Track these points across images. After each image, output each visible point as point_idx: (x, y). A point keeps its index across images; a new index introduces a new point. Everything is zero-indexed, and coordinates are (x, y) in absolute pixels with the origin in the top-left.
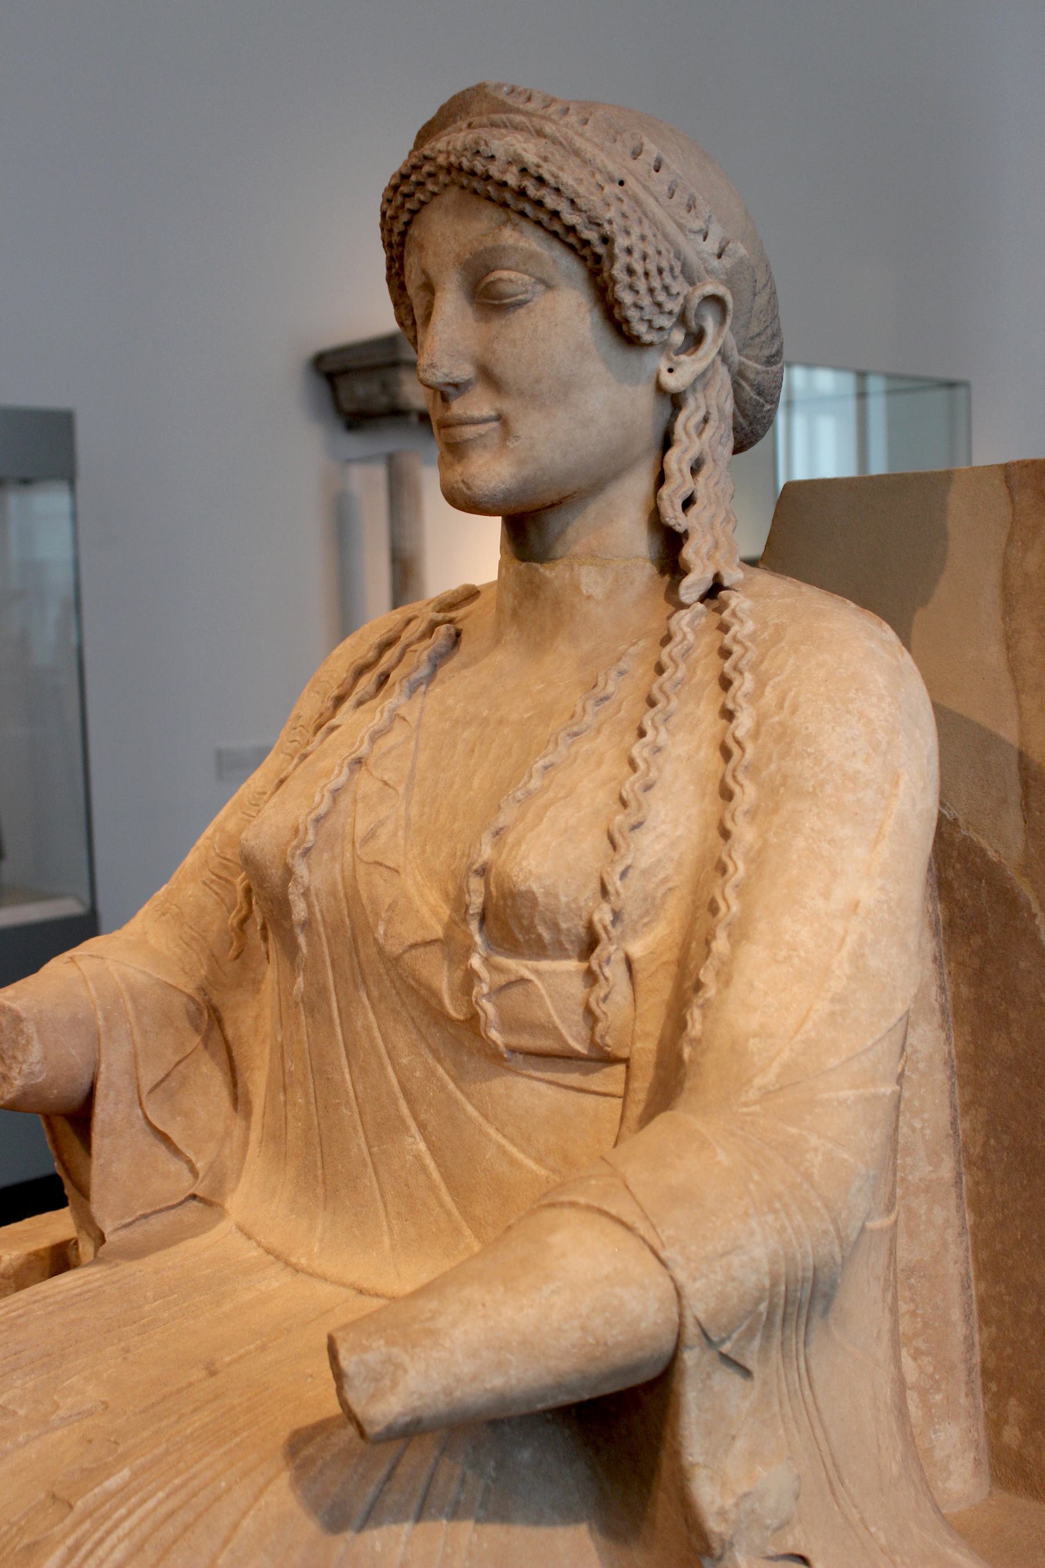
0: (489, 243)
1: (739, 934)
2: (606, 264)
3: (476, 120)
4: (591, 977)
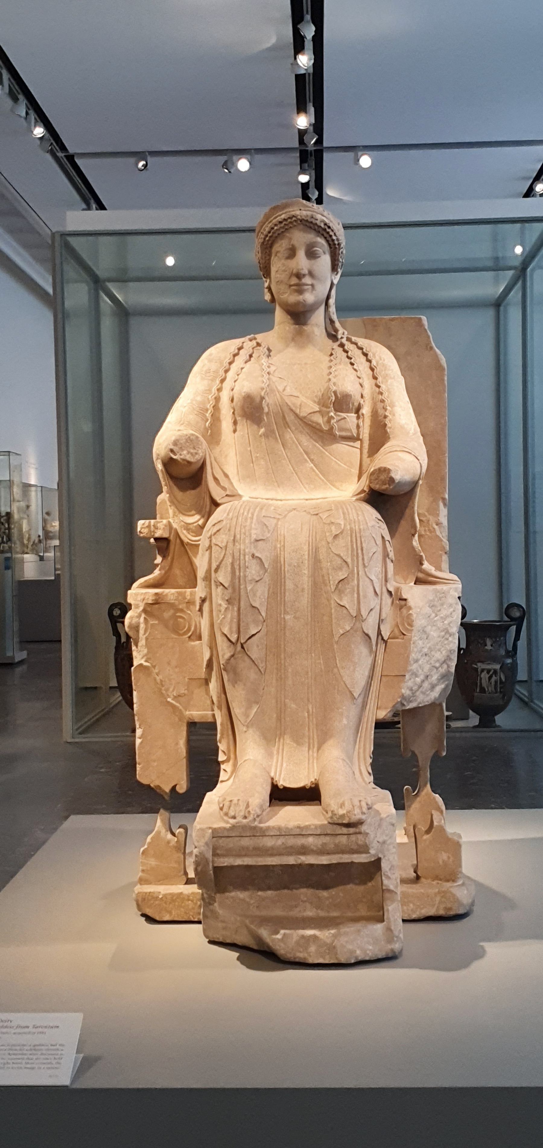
0: (314, 240)
1: (392, 406)
3: (302, 208)
4: (358, 418)
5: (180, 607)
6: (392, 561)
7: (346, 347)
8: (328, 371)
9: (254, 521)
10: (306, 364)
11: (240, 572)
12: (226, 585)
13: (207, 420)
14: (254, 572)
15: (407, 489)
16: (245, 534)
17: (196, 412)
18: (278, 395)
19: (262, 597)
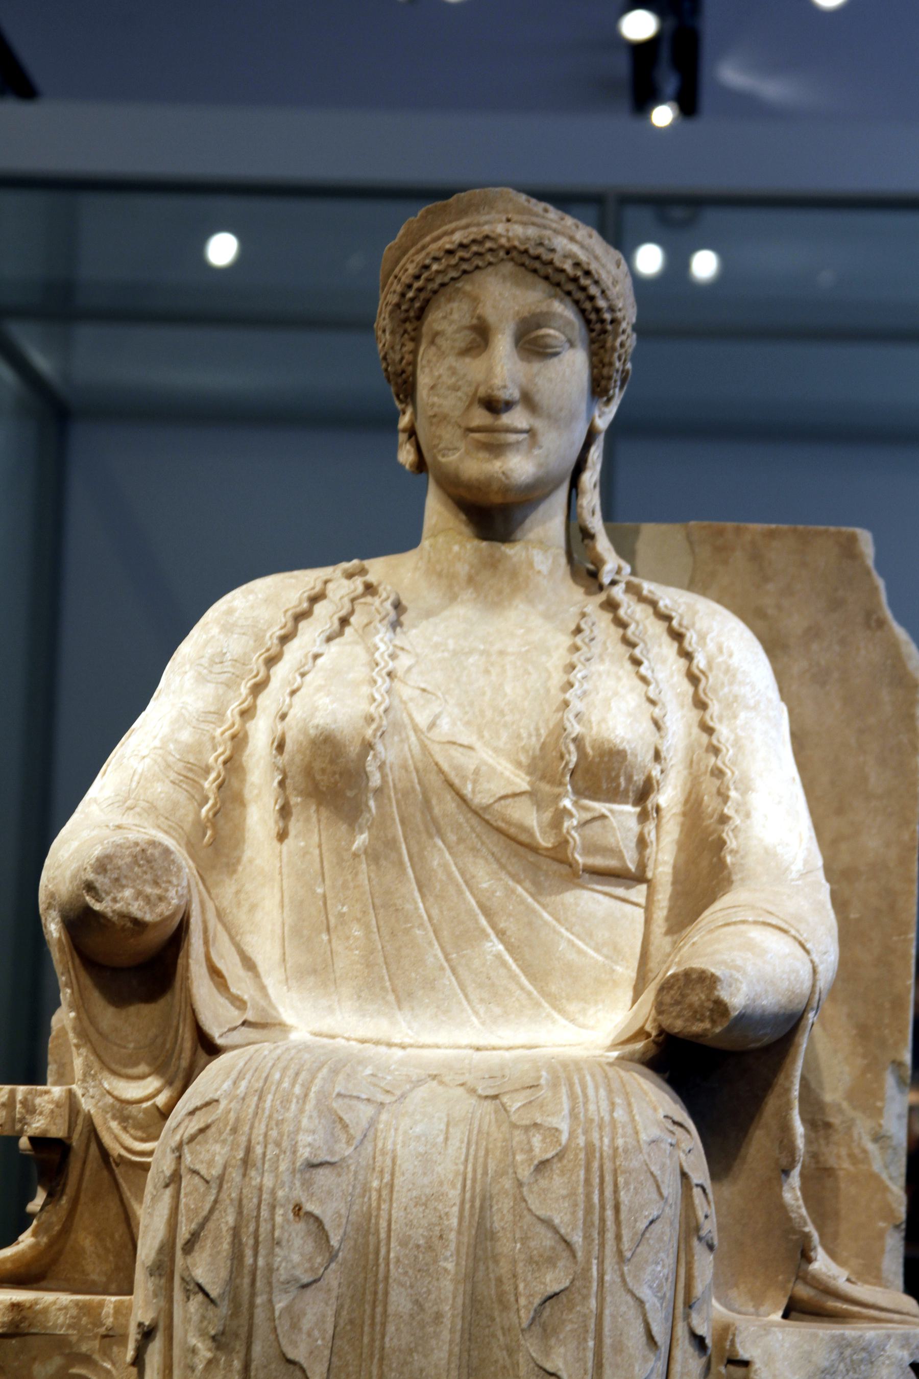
0: (543, 307)
1: (746, 788)
2: (610, 339)
3: (515, 217)
4: (643, 817)
5: (84, 1348)
6: (711, 1247)
7: (622, 612)
8: (565, 678)
9: (310, 1106)
10: (502, 653)
11: (256, 1255)
12: (214, 1294)
13: (206, 800)
14: (296, 1258)
15: (768, 1036)
16: (278, 1144)
17: (173, 776)
18: (413, 739)
19: (316, 1333)
